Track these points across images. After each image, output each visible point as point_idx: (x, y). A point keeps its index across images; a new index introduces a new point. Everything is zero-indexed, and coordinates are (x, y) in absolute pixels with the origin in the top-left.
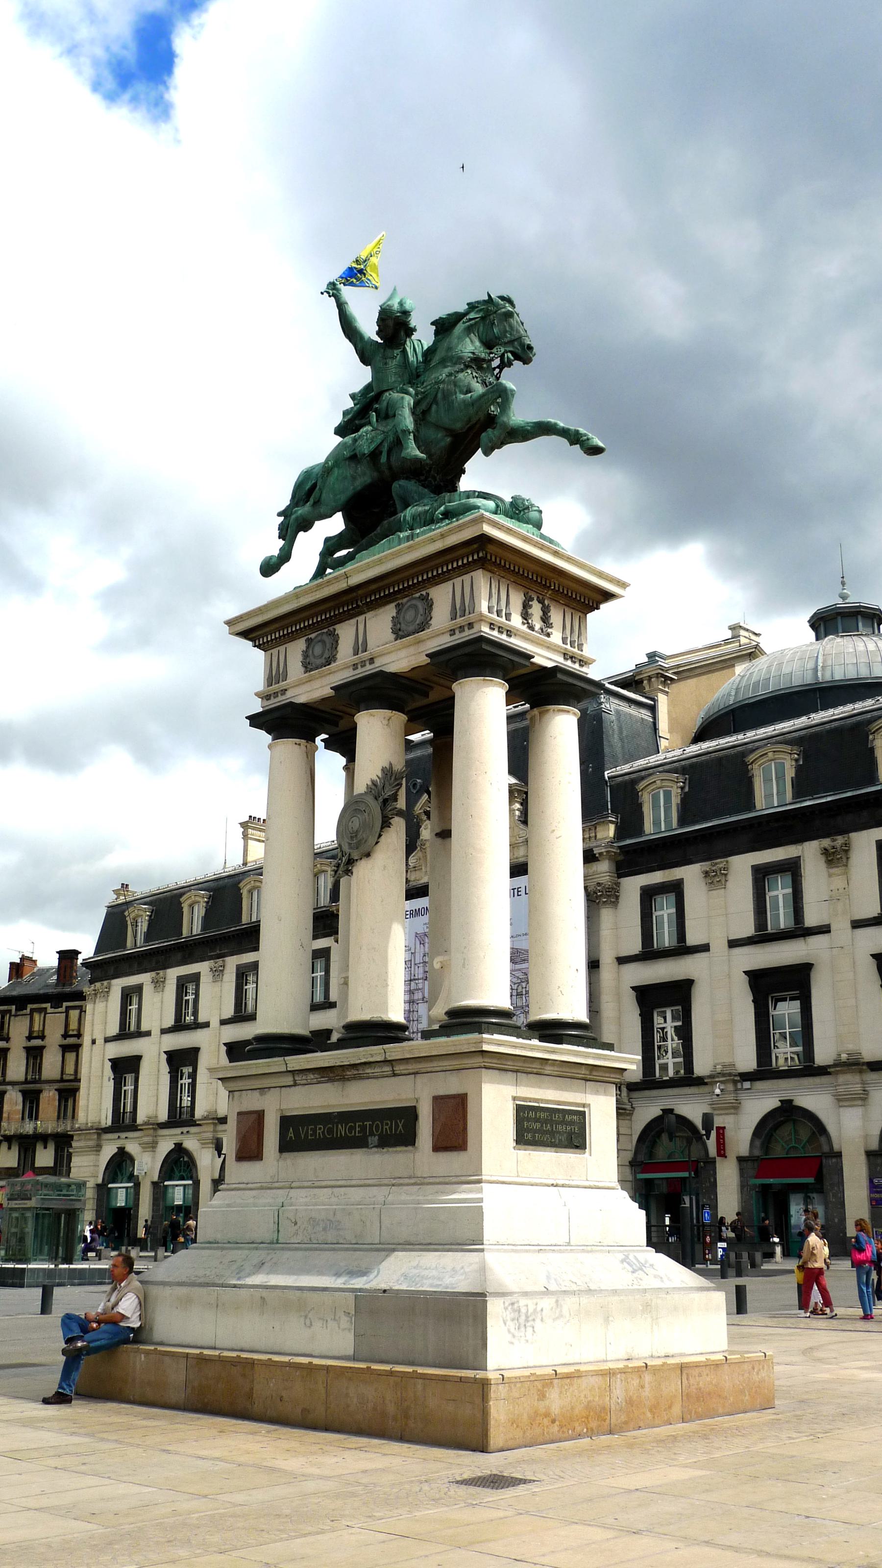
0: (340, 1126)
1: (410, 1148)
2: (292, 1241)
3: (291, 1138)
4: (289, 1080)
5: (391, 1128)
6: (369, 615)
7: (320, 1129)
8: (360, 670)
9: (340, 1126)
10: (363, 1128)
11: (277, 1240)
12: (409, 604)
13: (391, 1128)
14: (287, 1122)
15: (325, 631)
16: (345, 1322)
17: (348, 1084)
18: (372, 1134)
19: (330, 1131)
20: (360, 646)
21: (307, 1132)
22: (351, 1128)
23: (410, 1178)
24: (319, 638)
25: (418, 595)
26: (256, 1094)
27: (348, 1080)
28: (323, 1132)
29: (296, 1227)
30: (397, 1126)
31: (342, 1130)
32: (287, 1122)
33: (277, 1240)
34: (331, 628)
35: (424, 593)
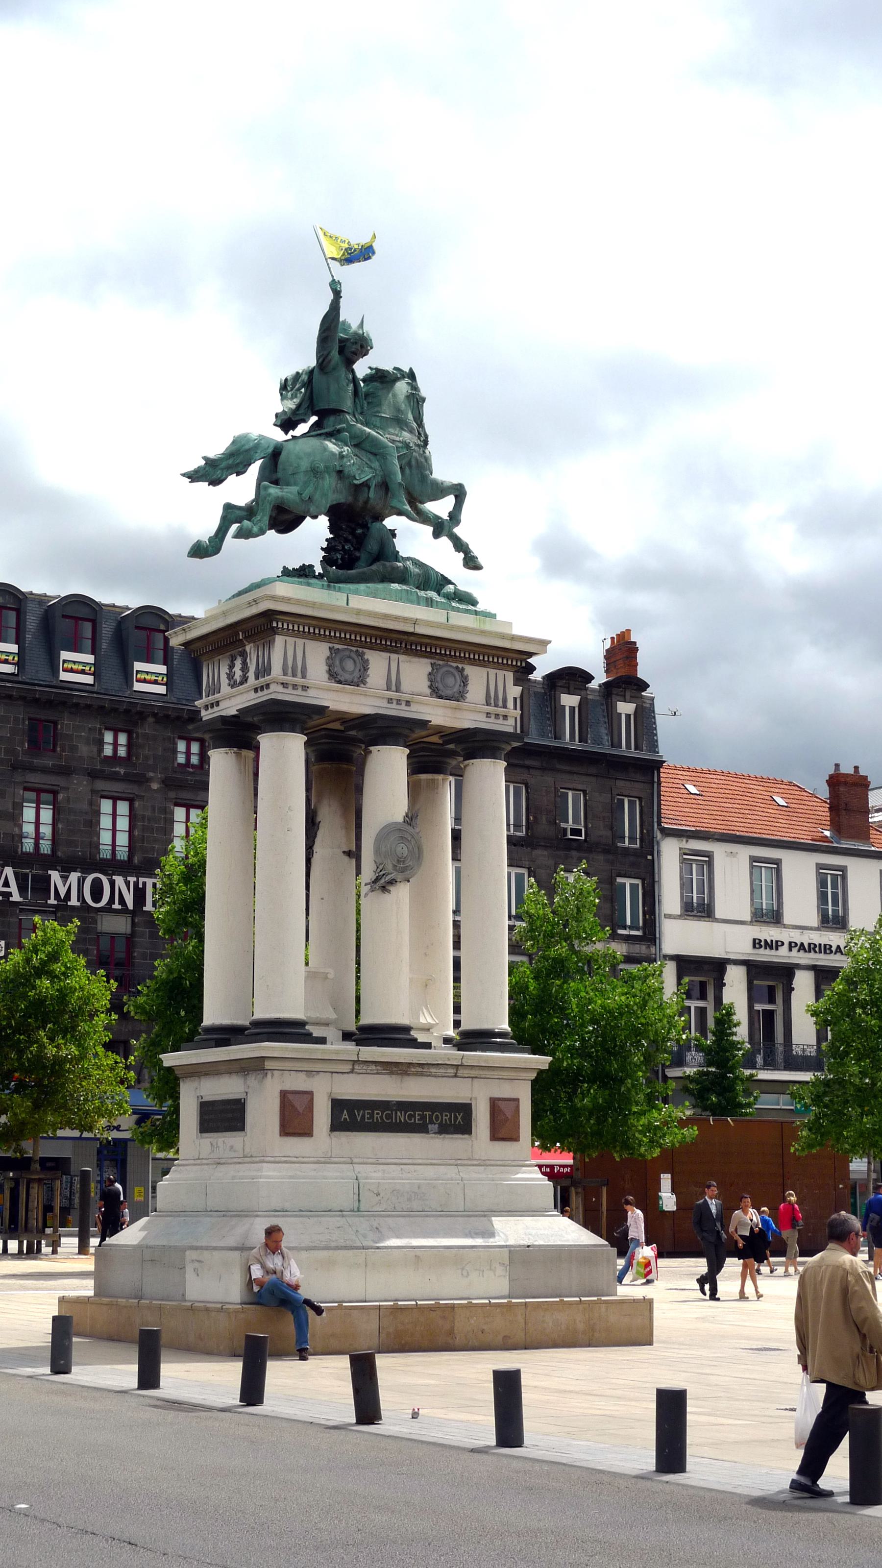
0: (399, 1113)
1: (466, 1136)
2: (375, 1209)
3: (346, 1119)
4: (347, 1068)
5: (450, 1119)
6: (402, 657)
7: (377, 1114)
8: (394, 706)
9: (399, 1113)
10: (423, 1117)
11: (358, 1208)
12: (445, 669)
13: (450, 1119)
14: (338, 1105)
15: (354, 649)
16: (500, 1271)
17: (406, 1078)
18: (431, 1122)
19: (389, 1117)
20: (394, 684)
21: (363, 1116)
22: (410, 1117)
23: (469, 1159)
24: (347, 653)
25: (454, 665)
26: (302, 1076)
27: (409, 1075)
28: (381, 1117)
29: (379, 1198)
30: (456, 1118)
31: (401, 1117)
32: (338, 1105)
33: (358, 1208)
34: (360, 650)
35: (460, 666)
